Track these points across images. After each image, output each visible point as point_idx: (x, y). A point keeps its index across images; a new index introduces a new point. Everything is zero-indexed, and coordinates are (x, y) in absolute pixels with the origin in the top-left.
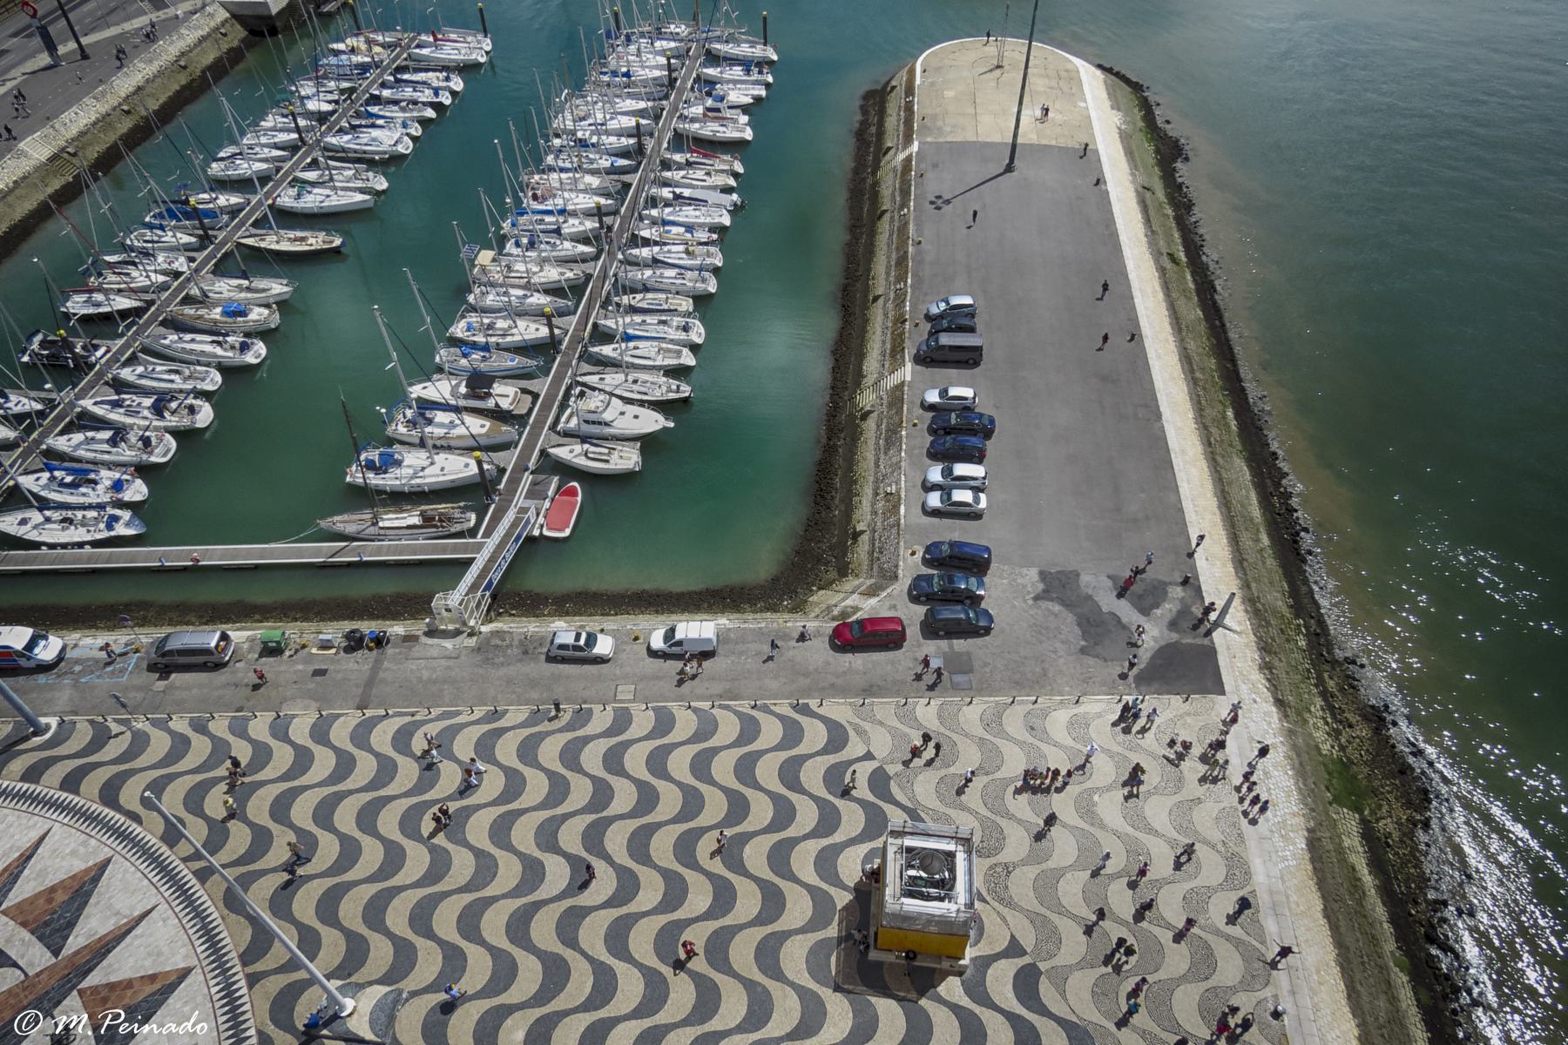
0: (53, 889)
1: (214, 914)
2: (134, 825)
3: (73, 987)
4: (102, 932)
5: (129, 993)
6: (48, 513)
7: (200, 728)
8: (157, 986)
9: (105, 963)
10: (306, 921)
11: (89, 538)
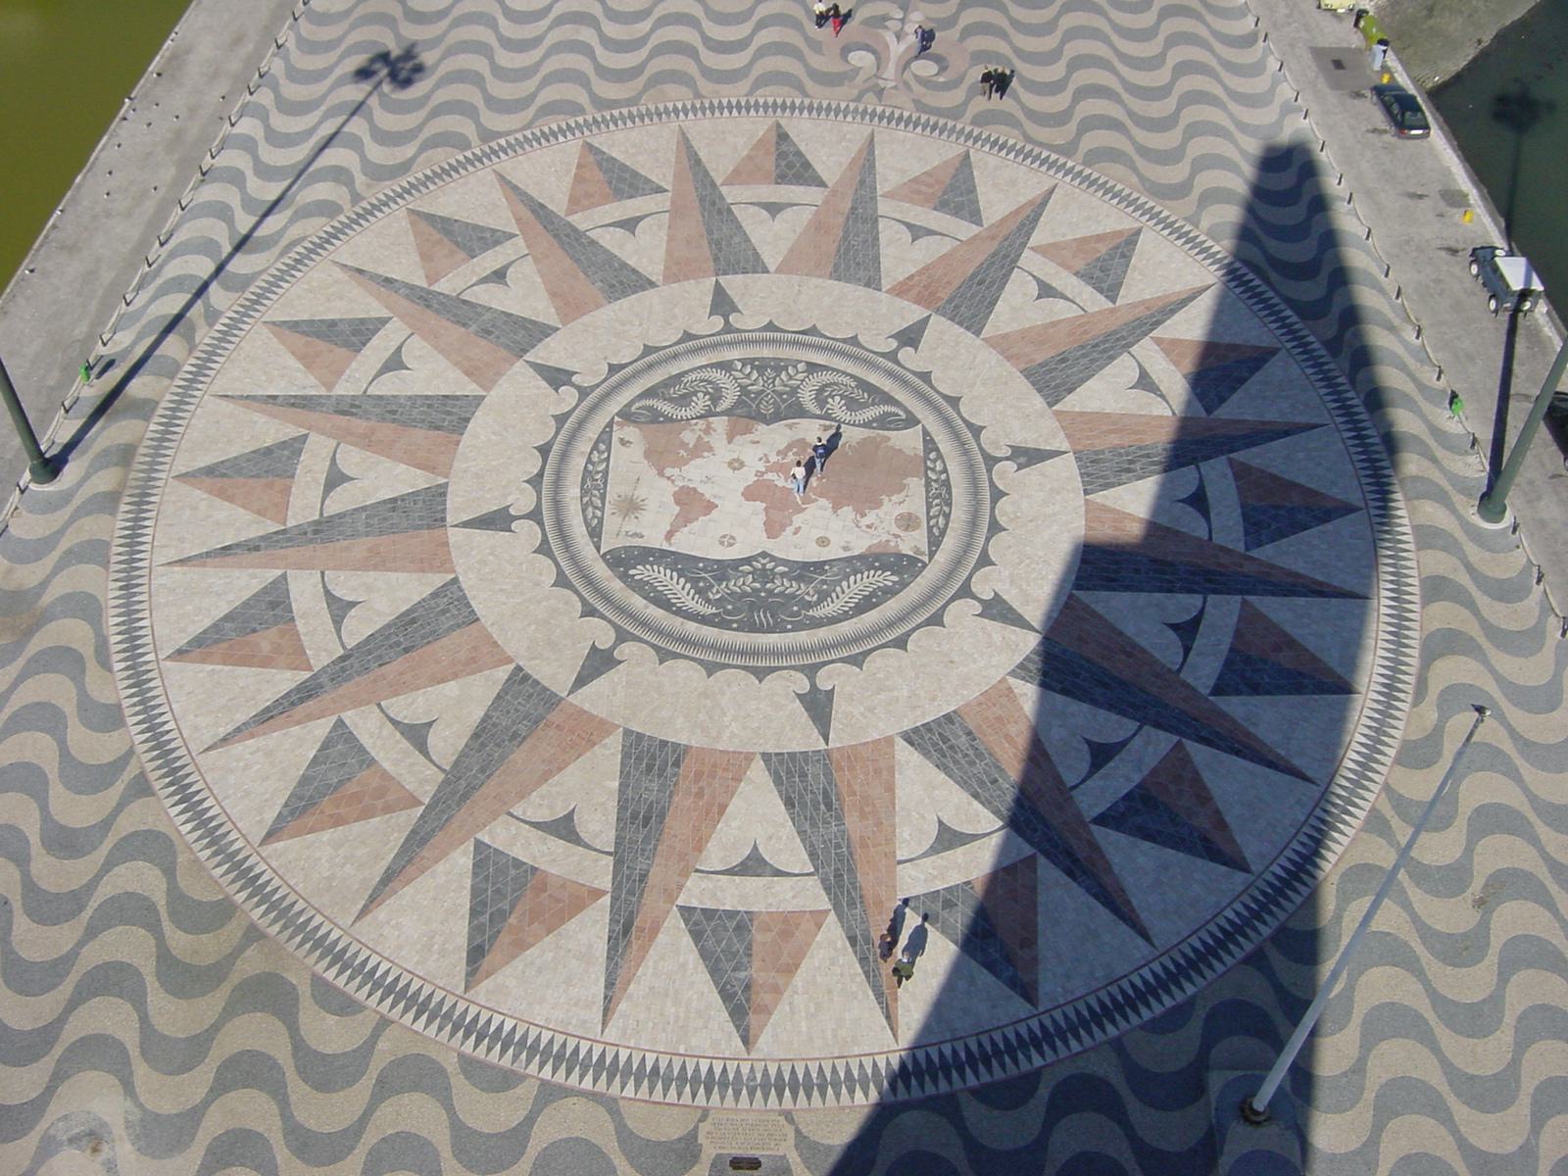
0: (1290, 643)
2: (1409, 699)
9: (1224, 756)
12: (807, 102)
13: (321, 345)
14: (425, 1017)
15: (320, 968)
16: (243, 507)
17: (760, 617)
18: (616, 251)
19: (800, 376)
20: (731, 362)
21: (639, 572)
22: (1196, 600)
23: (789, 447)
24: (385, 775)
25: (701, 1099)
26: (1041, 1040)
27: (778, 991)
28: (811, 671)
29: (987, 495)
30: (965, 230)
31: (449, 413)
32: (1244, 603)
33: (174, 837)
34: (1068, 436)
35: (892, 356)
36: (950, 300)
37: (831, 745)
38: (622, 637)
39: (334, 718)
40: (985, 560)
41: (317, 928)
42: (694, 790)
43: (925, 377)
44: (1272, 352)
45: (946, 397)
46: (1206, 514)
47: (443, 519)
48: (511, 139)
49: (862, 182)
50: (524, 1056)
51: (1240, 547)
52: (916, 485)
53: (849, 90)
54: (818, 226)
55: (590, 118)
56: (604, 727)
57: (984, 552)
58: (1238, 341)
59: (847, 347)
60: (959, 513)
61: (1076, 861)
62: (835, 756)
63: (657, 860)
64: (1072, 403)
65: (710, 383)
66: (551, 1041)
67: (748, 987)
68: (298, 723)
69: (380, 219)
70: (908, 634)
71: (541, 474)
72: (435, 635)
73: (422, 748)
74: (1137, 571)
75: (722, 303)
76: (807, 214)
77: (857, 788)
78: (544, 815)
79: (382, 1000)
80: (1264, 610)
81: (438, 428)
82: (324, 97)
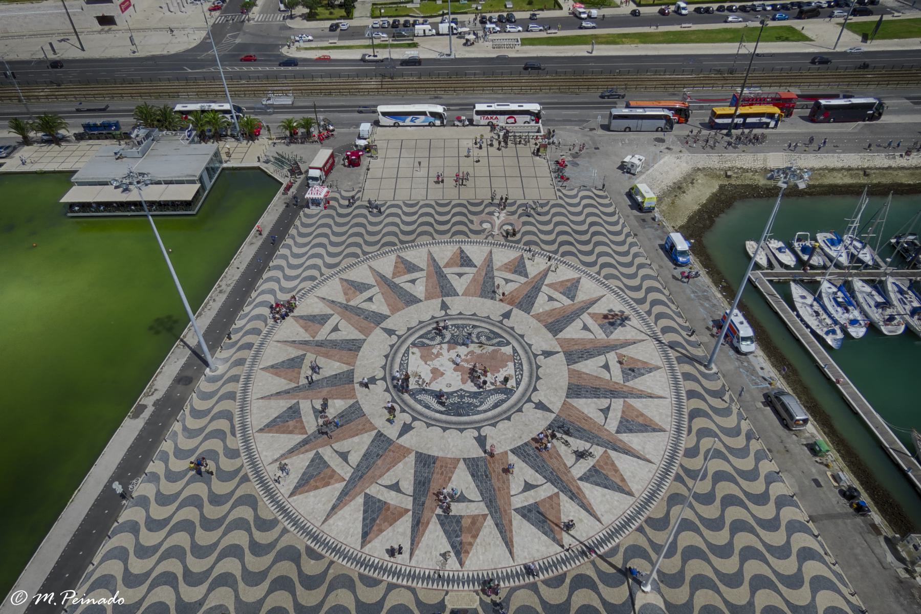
0: (642, 415)
1: (663, 493)
2: (685, 433)
3: (606, 447)
5: (613, 473)
6: (815, 303)
7: (749, 437)
8: (620, 484)
9: (621, 455)
10: (679, 543)
11: (814, 327)
13: (310, 323)
15: (309, 543)
16: (285, 379)
18: (408, 290)
21: (419, 397)
22: (608, 400)
23: (468, 354)
24: (334, 471)
25: (445, 587)
27: (471, 544)
28: (478, 429)
29: (535, 366)
30: (523, 280)
32: (624, 401)
33: (257, 496)
35: (501, 322)
36: (520, 303)
38: (414, 419)
39: (314, 452)
40: (535, 389)
41: (308, 527)
42: (440, 472)
43: (512, 328)
45: (519, 335)
49: (488, 266)
51: (622, 382)
52: (511, 365)
53: (483, 236)
54: (474, 280)
57: (535, 386)
60: (526, 374)
64: (560, 336)
66: (392, 567)
67: (461, 543)
69: (330, 282)
70: (511, 415)
71: (386, 365)
72: (351, 421)
73: (346, 460)
75: (444, 306)
78: (389, 483)
79: (331, 554)
81: (351, 350)
82: (310, 242)
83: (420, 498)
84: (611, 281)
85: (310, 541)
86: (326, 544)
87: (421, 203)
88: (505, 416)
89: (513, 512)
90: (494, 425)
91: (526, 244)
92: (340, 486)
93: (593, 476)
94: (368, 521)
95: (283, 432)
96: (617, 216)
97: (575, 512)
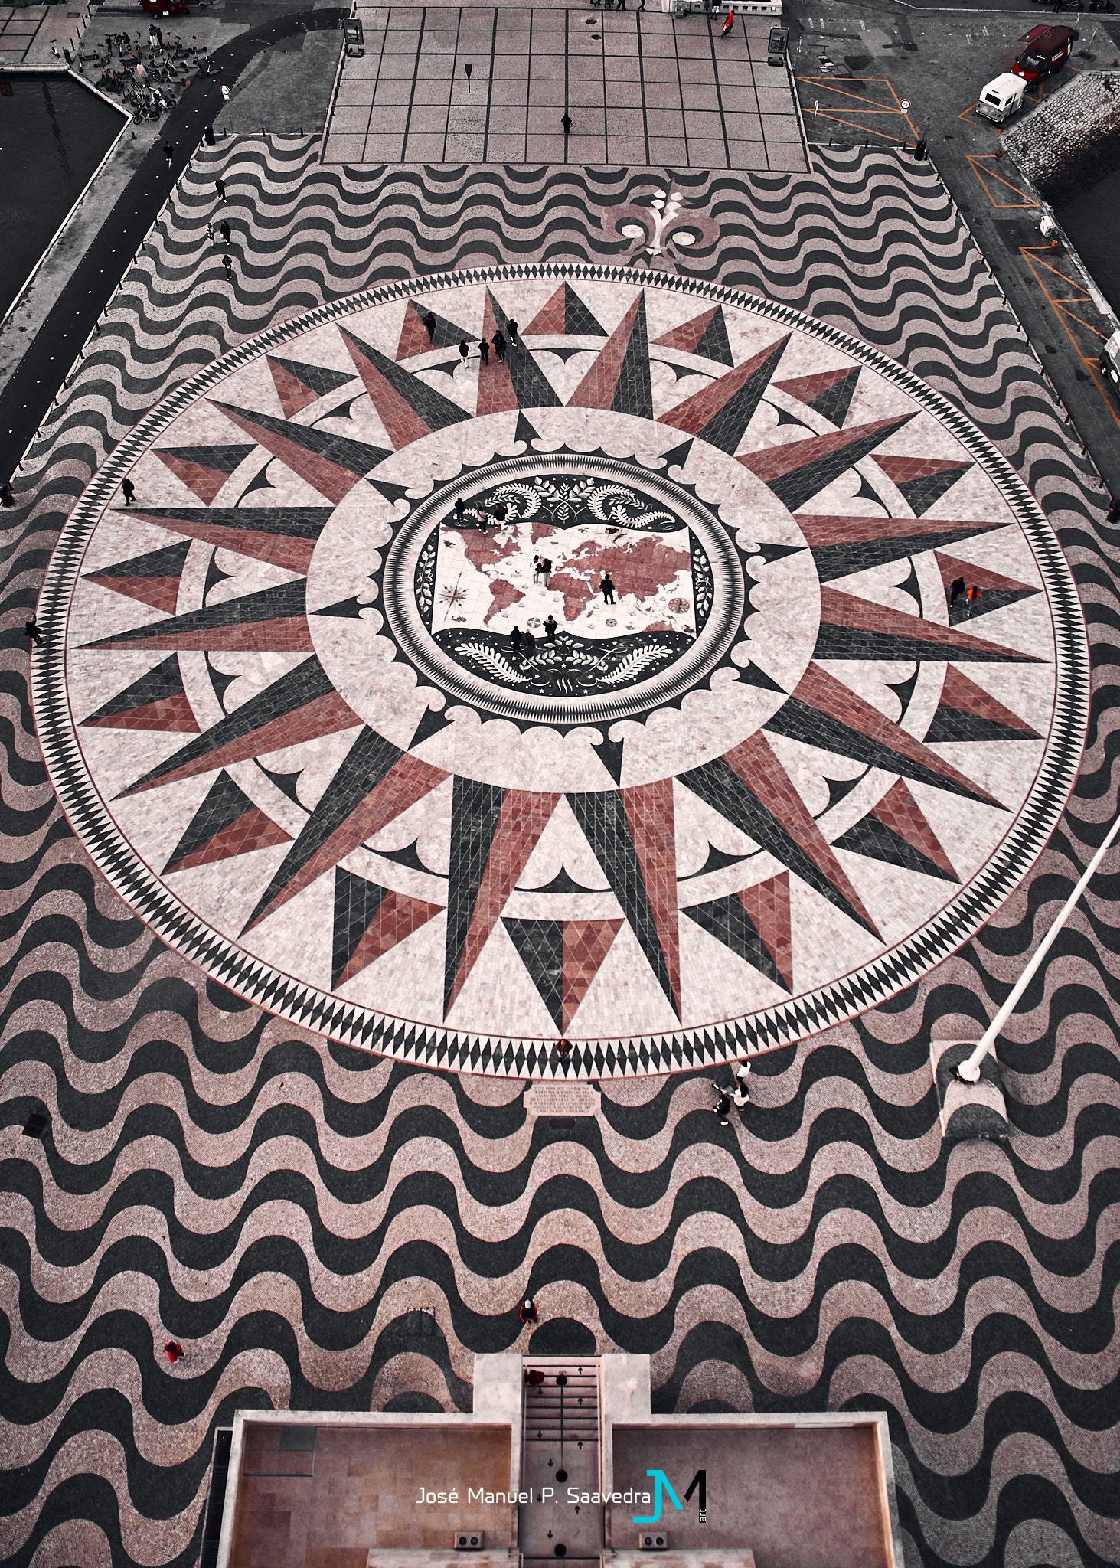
0: (987, 699)
2: (1082, 742)
4: (963, 770)
5: (914, 830)
8: (929, 854)
12: (590, 266)
14: (300, 1010)
15: (214, 973)
17: (563, 684)
19: (589, 489)
20: (533, 478)
21: (466, 649)
22: (912, 665)
23: (582, 547)
24: (263, 817)
25: (525, 1073)
26: (791, 1021)
27: (583, 984)
28: (604, 727)
29: (742, 580)
30: (719, 370)
31: (305, 522)
34: (806, 535)
35: (663, 472)
36: (709, 426)
37: (622, 786)
38: (451, 701)
39: (218, 772)
40: (741, 636)
41: (211, 941)
42: (512, 823)
43: (690, 488)
44: (968, 466)
46: (918, 597)
47: (304, 608)
48: (350, 298)
49: (635, 332)
50: (381, 1040)
51: (945, 623)
52: (684, 576)
54: (598, 368)
55: (413, 281)
56: (435, 775)
57: (741, 628)
58: (940, 458)
59: (625, 465)
60: (720, 597)
61: (820, 876)
62: (626, 794)
63: (485, 881)
65: (517, 495)
66: (403, 1028)
68: (190, 775)
69: (244, 367)
72: (300, 702)
74: (864, 643)
75: (525, 431)
76: (593, 356)
77: (643, 820)
78: (392, 847)
79: (264, 998)
80: (967, 674)
81: (298, 534)
83: (466, 882)
84: (933, 379)
85: (217, 969)
86: (251, 978)
87: (471, 171)
88: (666, 698)
89: (681, 915)
90: (641, 718)
91: (730, 280)
92: (280, 852)
93: (867, 836)
94: (347, 931)
95: (144, 726)
96: (953, 217)
97: (823, 916)
